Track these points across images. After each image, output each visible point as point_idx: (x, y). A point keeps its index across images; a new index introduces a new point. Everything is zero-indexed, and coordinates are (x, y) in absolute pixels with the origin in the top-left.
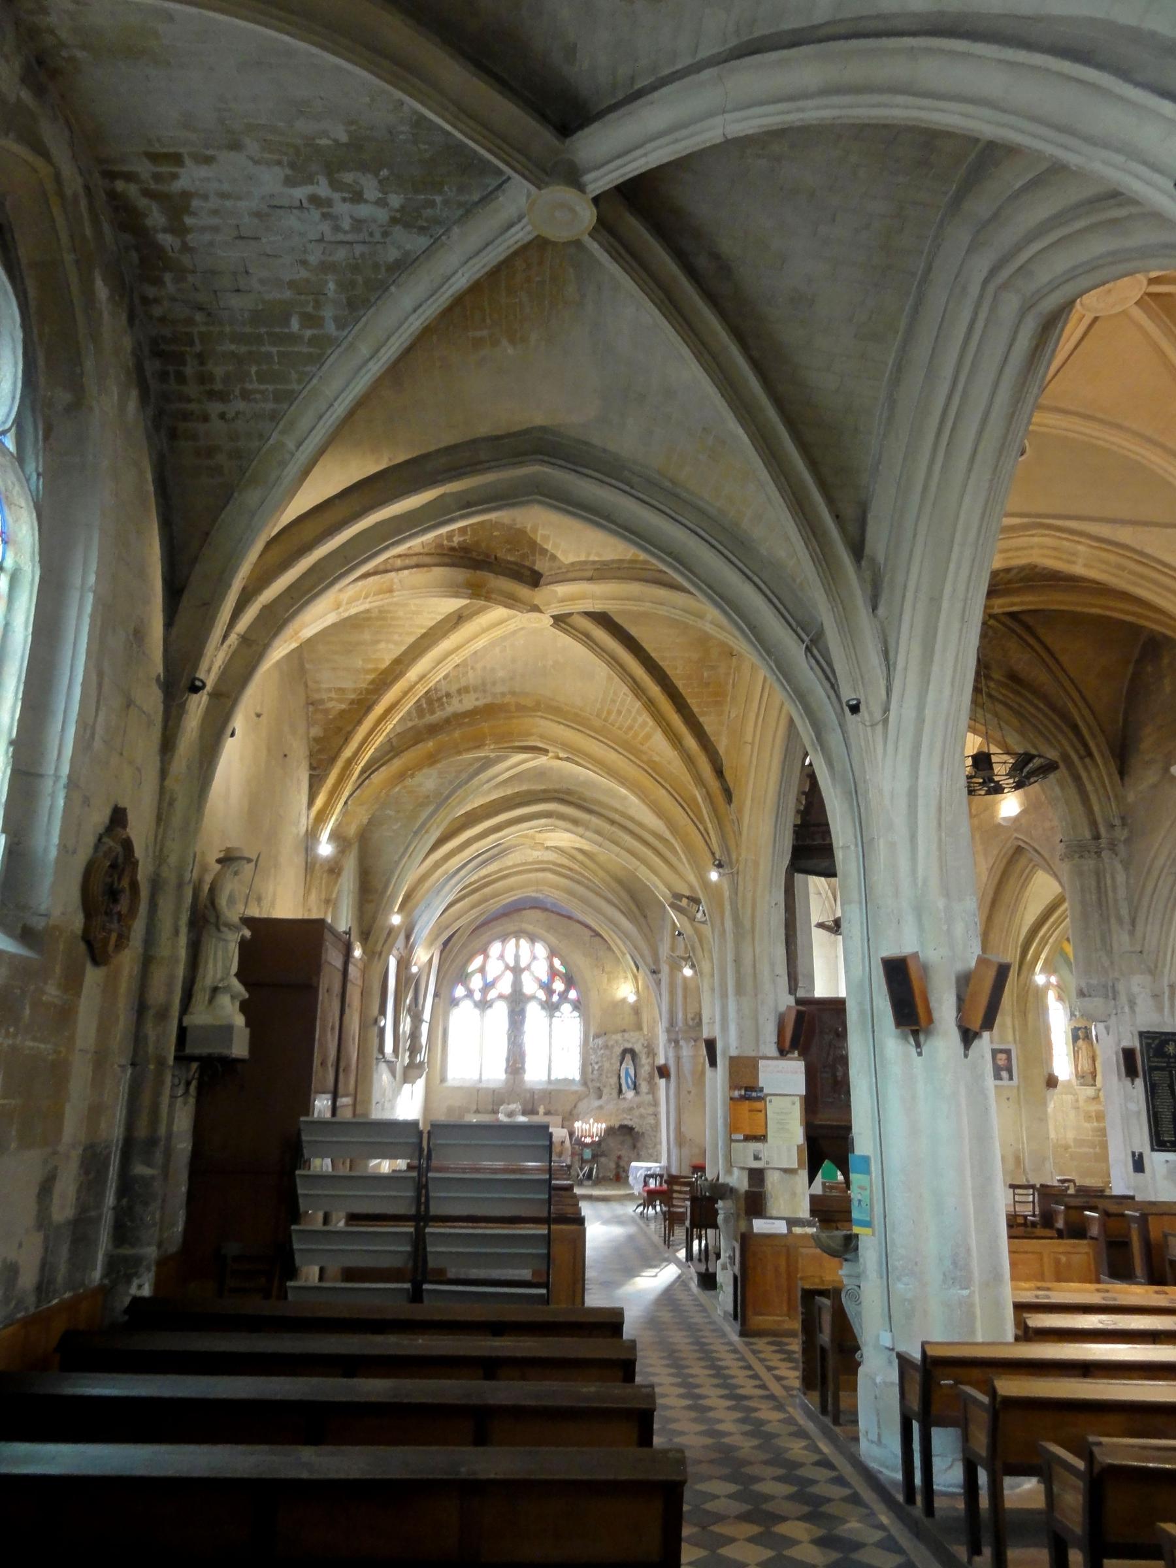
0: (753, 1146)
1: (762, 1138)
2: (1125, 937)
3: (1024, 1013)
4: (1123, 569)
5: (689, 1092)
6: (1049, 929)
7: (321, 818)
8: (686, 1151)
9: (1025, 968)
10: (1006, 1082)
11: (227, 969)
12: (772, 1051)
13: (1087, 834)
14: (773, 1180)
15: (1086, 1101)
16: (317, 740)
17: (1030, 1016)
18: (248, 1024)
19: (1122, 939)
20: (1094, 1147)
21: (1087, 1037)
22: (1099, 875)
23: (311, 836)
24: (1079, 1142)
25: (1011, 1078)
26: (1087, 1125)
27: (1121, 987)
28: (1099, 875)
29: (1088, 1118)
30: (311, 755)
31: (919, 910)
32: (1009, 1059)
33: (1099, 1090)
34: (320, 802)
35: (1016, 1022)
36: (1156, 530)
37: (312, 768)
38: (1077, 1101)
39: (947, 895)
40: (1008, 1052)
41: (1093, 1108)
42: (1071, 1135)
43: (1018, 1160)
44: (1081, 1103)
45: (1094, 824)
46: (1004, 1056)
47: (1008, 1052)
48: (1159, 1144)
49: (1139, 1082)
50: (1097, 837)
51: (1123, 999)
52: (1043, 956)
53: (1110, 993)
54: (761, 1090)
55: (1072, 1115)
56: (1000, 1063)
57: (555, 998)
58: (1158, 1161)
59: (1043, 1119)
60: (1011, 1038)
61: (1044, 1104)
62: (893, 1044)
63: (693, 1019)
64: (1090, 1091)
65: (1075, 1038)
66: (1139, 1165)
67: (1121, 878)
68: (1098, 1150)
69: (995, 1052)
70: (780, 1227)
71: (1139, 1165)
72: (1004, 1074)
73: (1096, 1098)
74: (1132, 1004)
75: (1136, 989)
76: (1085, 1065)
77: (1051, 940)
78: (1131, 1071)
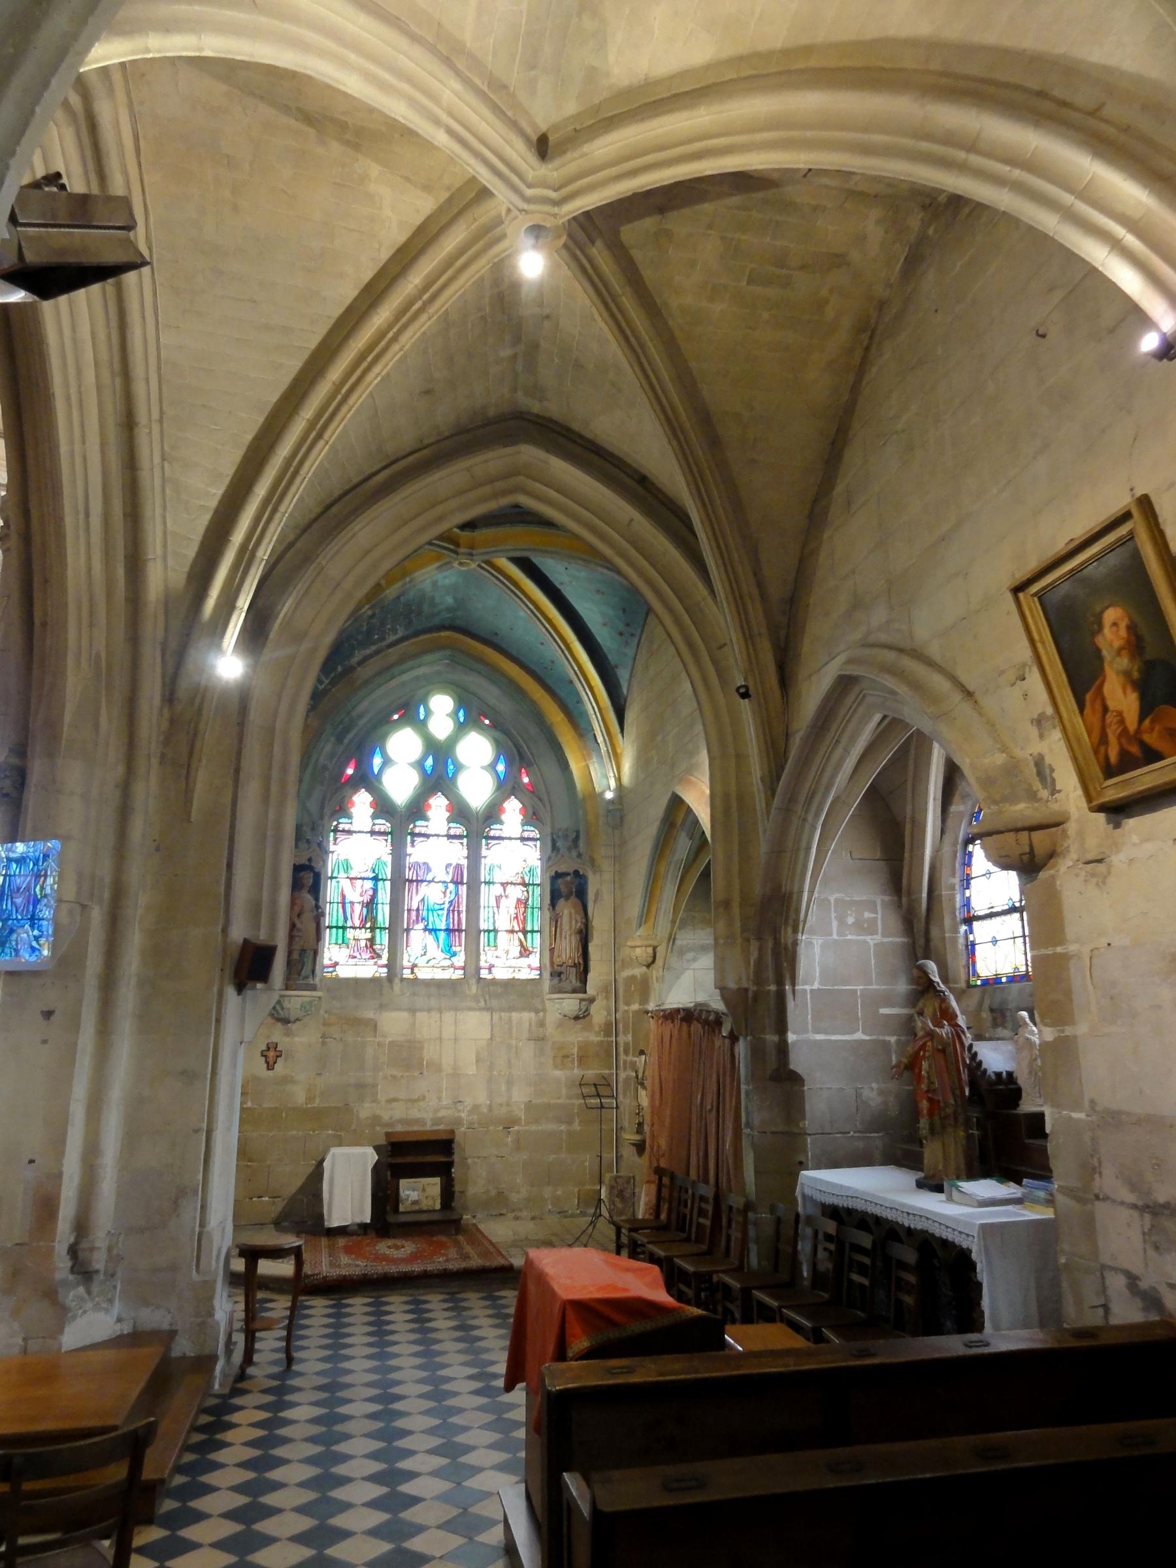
15: (560, 1025)
20: (570, 1123)
21: (581, 893)
24: (535, 1111)
26: (558, 1073)
29: (562, 1058)
33: (592, 1000)
38: (541, 1024)
41: (576, 1037)
42: (520, 1096)
44: (550, 1029)
55: (528, 1052)
64: (570, 1003)
65: (555, 897)
68: (576, 1126)
73: (581, 1017)
76: (568, 949)
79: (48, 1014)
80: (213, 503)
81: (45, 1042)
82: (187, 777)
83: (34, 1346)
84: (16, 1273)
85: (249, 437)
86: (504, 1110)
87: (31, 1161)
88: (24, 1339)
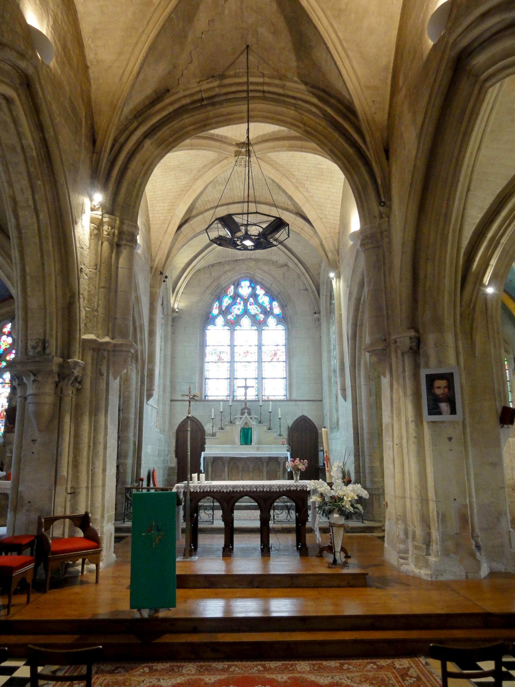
3: (469, 334)
5: (34, 441)
6: (500, 227)
8: (22, 517)
9: (471, 279)
10: (446, 417)
17: (478, 338)
25: (453, 411)
32: (451, 386)
35: (460, 344)
40: (449, 377)
43: (464, 519)
47: (449, 377)
52: (493, 262)
56: (438, 392)
59: (497, 464)
60: (452, 361)
61: (497, 444)
63: (34, 348)
69: (431, 379)
72: (444, 406)
77: (504, 240)
79: (450, 439)
80: (477, 221)
81: (451, 450)
82: (471, 338)
83: (470, 576)
84: (458, 546)
85: (498, 191)
86: (511, 482)
87: (455, 500)
88: (466, 573)
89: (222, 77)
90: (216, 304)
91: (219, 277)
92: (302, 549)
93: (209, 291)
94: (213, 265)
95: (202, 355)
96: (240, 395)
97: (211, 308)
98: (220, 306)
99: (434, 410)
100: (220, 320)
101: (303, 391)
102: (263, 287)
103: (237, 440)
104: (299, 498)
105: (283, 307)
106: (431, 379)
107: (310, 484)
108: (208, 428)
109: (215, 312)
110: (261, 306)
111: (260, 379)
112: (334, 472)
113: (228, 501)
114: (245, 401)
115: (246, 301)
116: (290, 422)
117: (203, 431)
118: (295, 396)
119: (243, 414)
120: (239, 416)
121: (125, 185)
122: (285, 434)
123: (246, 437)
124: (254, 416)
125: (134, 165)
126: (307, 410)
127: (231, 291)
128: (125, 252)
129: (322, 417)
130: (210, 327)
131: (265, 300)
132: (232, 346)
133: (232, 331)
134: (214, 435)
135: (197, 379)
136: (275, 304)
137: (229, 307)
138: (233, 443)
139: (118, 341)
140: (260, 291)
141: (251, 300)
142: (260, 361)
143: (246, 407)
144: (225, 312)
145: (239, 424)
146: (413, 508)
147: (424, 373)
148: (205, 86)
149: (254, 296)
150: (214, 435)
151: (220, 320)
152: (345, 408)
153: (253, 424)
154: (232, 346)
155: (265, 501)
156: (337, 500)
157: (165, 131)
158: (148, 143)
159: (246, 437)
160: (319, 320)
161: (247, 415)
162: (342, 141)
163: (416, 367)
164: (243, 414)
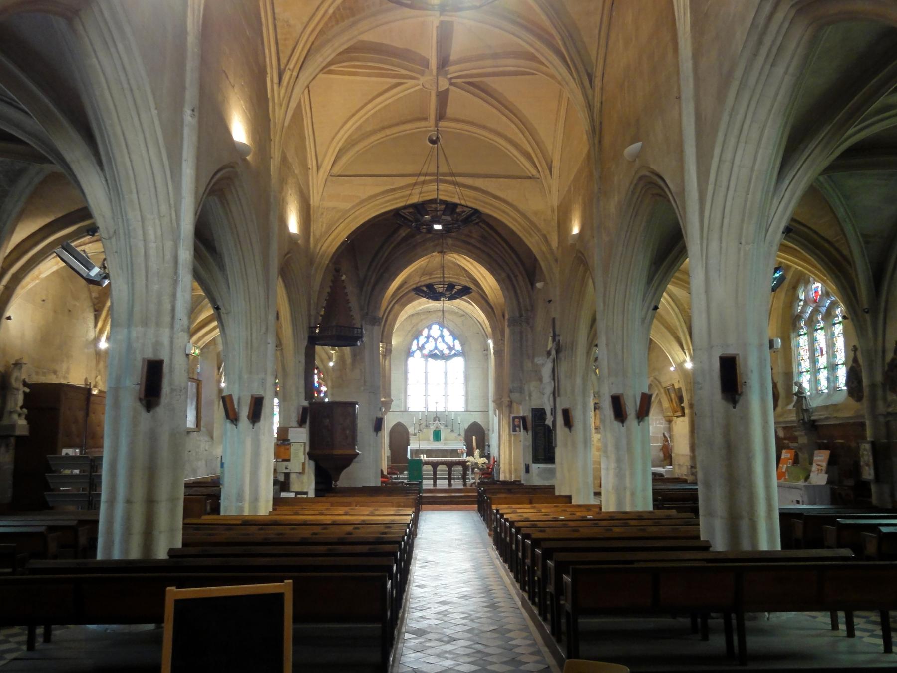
0: (285, 463)
1: (288, 460)
2: (530, 365)
4: (477, 200)
7: (101, 331)
11: (16, 404)
12: (295, 424)
13: (518, 315)
14: (293, 477)
16: (96, 298)
18: (28, 423)
19: (528, 365)
22: (521, 333)
23: (97, 339)
27: (526, 388)
28: (521, 333)
30: (94, 304)
31: (240, 378)
34: (100, 325)
36: (494, 180)
37: (96, 310)
39: (250, 373)
45: (520, 310)
46: (517, 420)
48: (536, 460)
49: (530, 433)
50: (521, 316)
51: (527, 393)
53: (521, 391)
54: (288, 440)
57: (322, 395)
58: (535, 467)
62: (229, 425)
66: (527, 470)
67: (529, 336)
70: (292, 495)
71: (527, 470)
74: (530, 396)
75: (532, 389)
78: (525, 428)
89: (431, 274)
90: (415, 342)
91: (417, 324)
92: (465, 484)
93: (410, 334)
94: (412, 315)
95: (406, 379)
96: (432, 409)
97: (411, 344)
98: (418, 345)
99: (514, 430)
100: (418, 354)
101: (476, 405)
102: (449, 330)
103: (431, 437)
104: (463, 464)
105: (462, 345)
106: (514, 418)
107: (469, 458)
108: (411, 430)
109: (414, 347)
110: (447, 344)
111: (446, 396)
112: (477, 452)
113: (435, 465)
114: (436, 412)
115: (436, 340)
116: (466, 426)
117: (407, 433)
118: (471, 408)
119: (434, 421)
120: (432, 422)
121: (387, 326)
122: (463, 433)
123: (437, 436)
124: (442, 422)
125: (391, 317)
126: (478, 418)
127: (425, 332)
128: (388, 358)
129: (488, 423)
130: (410, 360)
131: (449, 339)
132: (426, 373)
133: (426, 361)
134: (415, 434)
135: (403, 397)
136: (457, 343)
137: (423, 346)
138: (429, 440)
139: (388, 400)
140: (446, 333)
141: (440, 340)
142: (446, 383)
143: (437, 417)
144: (421, 348)
145: (432, 428)
146: (507, 467)
147: (512, 415)
148: (423, 279)
149: (442, 336)
150: (415, 434)
151: (418, 354)
152: (496, 420)
153: (442, 427)
154: (426, 373)
155: (450, 465)
156: (477, 463)
157: (405, 299)
158: (396, 306)
159: (437, 436)
160: (487, 355)
161: (437, 423)
162: (485, 304)
163: (510, 412)
164: (434, 421)
